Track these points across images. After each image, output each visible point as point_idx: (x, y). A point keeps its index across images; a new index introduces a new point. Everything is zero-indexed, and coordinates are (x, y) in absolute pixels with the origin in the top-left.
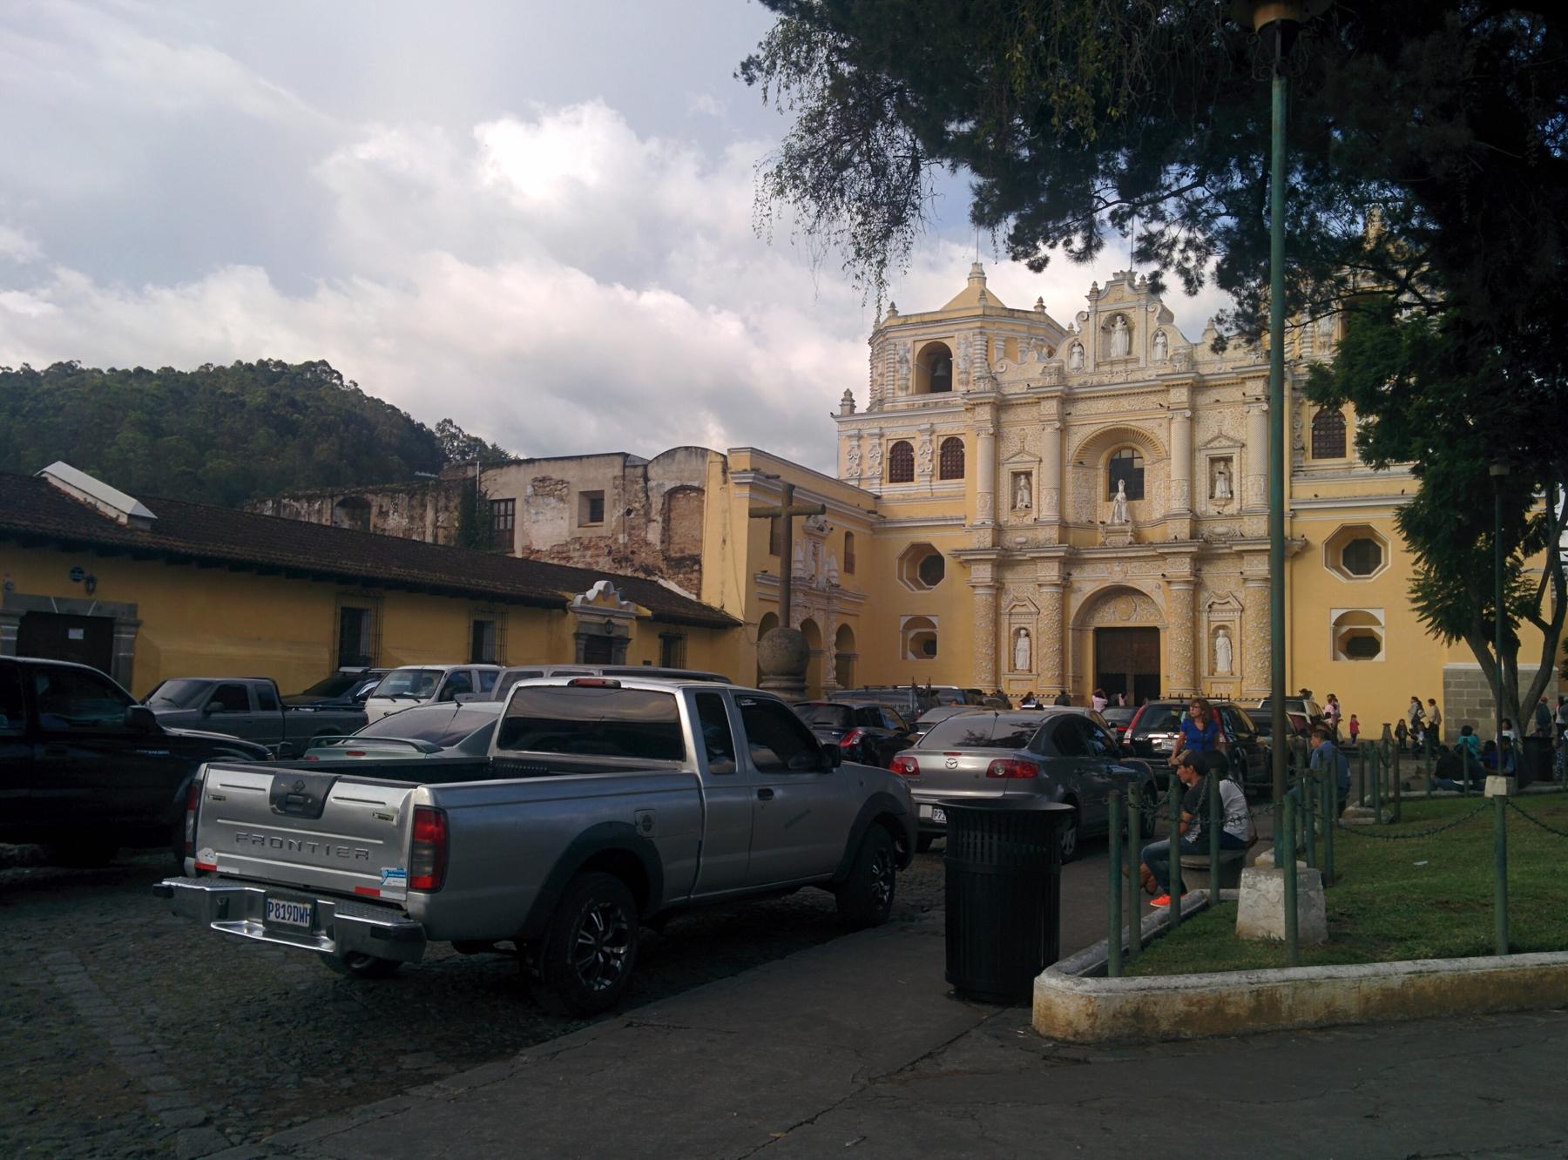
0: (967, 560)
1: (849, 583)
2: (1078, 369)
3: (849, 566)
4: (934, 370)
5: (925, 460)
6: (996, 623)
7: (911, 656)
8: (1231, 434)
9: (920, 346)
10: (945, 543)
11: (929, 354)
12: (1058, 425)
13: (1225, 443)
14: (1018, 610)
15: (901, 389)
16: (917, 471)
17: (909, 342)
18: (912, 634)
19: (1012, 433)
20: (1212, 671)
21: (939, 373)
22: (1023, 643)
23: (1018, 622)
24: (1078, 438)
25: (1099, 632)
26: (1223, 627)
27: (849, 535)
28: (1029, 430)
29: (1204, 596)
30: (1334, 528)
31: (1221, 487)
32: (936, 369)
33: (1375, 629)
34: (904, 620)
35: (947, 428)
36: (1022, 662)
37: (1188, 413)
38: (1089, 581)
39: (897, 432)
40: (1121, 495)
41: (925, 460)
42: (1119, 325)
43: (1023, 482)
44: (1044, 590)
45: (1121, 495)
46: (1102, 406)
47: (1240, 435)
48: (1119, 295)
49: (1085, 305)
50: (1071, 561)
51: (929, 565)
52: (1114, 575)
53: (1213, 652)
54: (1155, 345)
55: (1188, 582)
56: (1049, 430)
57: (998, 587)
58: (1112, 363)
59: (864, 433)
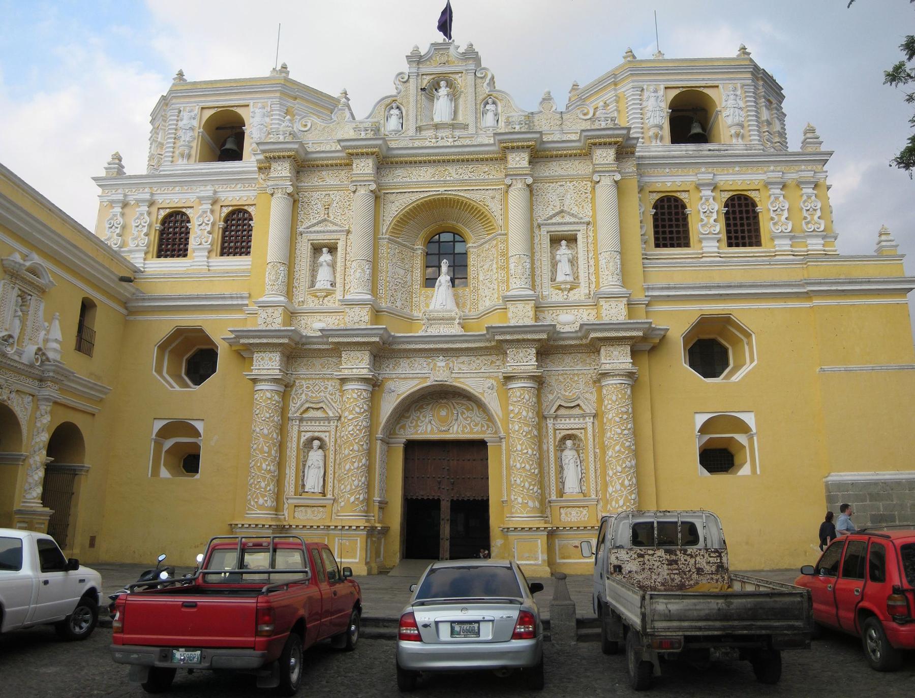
0: (245, 350)
1: (76, 364)
2: (397, 132)
3: (84, 341)
4: (224, 144)
5: (203, 232)
6: (282, 429)
7: (164, 473)
8: (575, 210)
9: (208, 114)
10: (219, 329)
11: (217, 129)
12: (373, 187)
13: (568, 219)
14: (311, 414)
15: (182, 156)
16: (193, 243)
17: (197, 110)
18: (168, 444)
19: (316, 202)
20: (561, 493)
21: (229, 145)
22: (315, 456)
23: (311, 429)
24: (395, 208)
25: (411, 446)
26: (569, 437)
27: (87, 306)
28: (336, 196)
29: (552, 399)
30: (694, 319)
31: (564, 269)
32: (225, 138)
33: (741, 438)
34: (158, 425)
35: (234, 196)
36: (313, 481)
37: (530, 181)
38: (406, 379)
39: (172, 199)
40: (444, 278)
41: (203, 232)
42: (443, 91)
43: (325, 257)
44: (349, 386)
45: (444, 278)
46: (423, 175)
47: (586, 213)
48: (444, 59)
49: (405, 68)
50: (384, 351)
51: (197, 358)
52: (438, 372)
53: (561, 469)
54: (484, 113)
55: (533, 378)
56: (362, 191)
57: (286, 387)
58: (437, 127)
59: (131, 199)
